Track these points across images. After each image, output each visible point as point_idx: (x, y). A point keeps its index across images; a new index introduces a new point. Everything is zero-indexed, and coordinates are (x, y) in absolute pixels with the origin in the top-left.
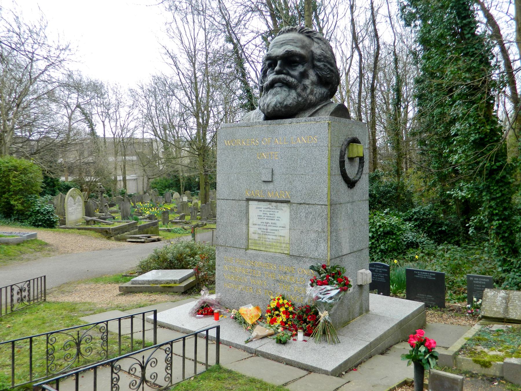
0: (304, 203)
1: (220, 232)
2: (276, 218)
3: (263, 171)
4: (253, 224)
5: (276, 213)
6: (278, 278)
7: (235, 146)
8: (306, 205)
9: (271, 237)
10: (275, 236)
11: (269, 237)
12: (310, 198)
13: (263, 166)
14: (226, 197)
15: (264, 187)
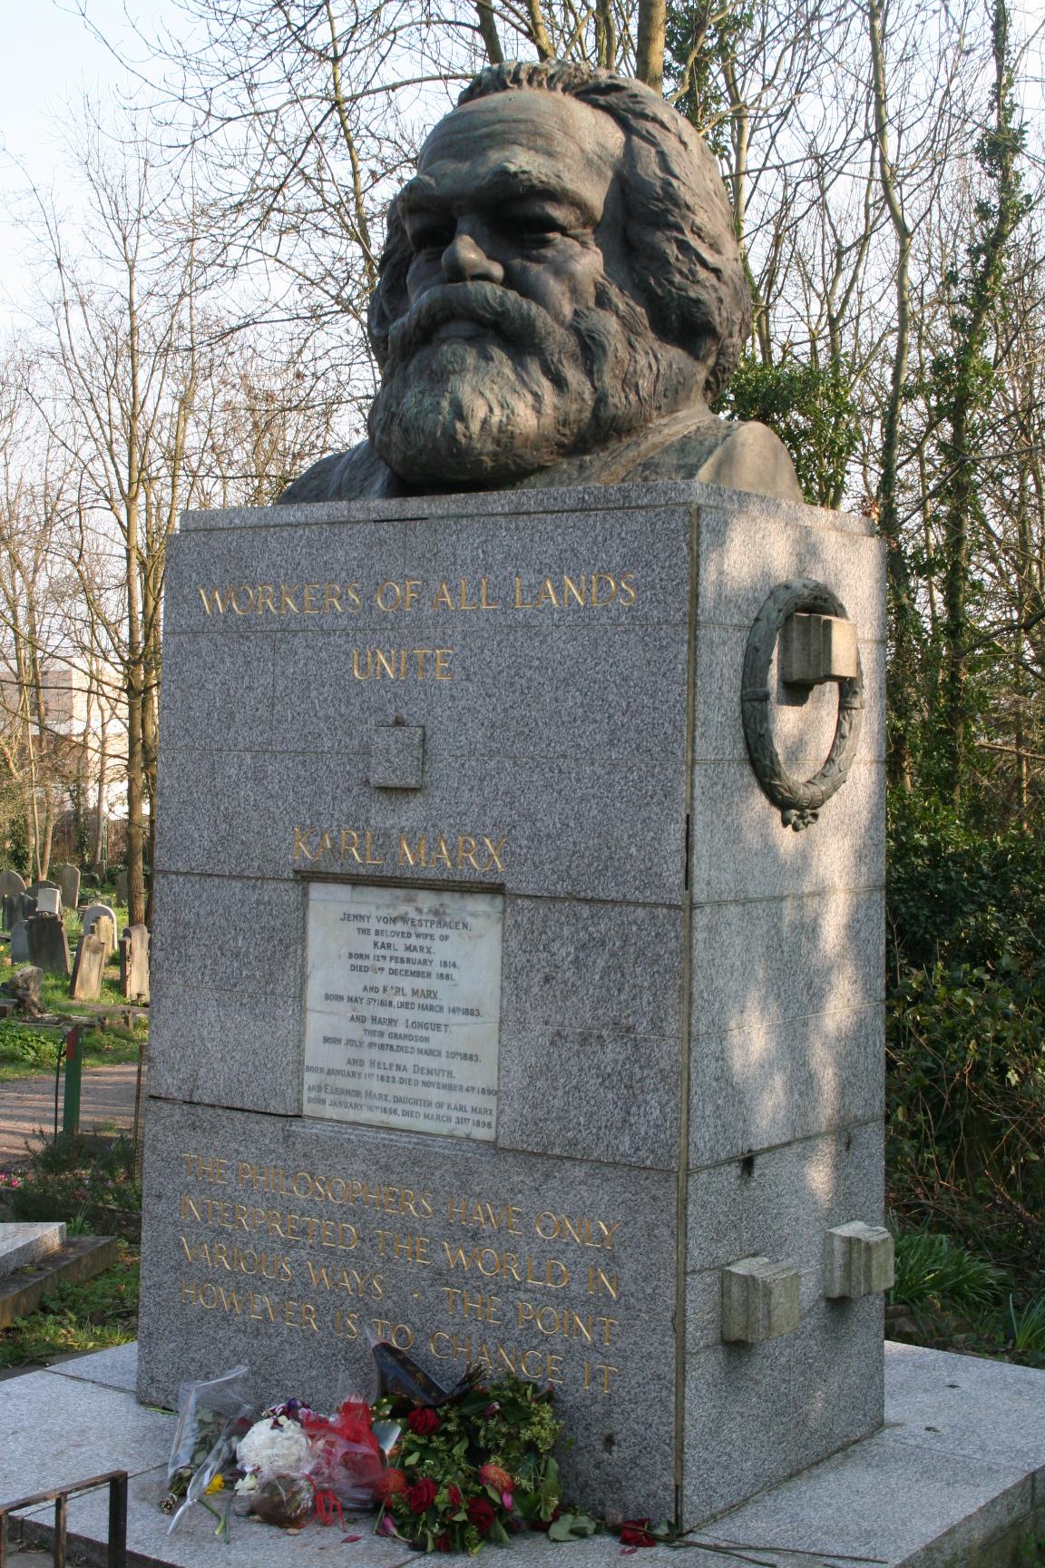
0: (573, 898)
2: (436, 969)
4: (327, 997)
5: (436, 944)
7: (246, 619)
9: (408, 1060)
10: (430, 1053)
12: (600, 873)
13: (380, 716)
15: (382, 816)
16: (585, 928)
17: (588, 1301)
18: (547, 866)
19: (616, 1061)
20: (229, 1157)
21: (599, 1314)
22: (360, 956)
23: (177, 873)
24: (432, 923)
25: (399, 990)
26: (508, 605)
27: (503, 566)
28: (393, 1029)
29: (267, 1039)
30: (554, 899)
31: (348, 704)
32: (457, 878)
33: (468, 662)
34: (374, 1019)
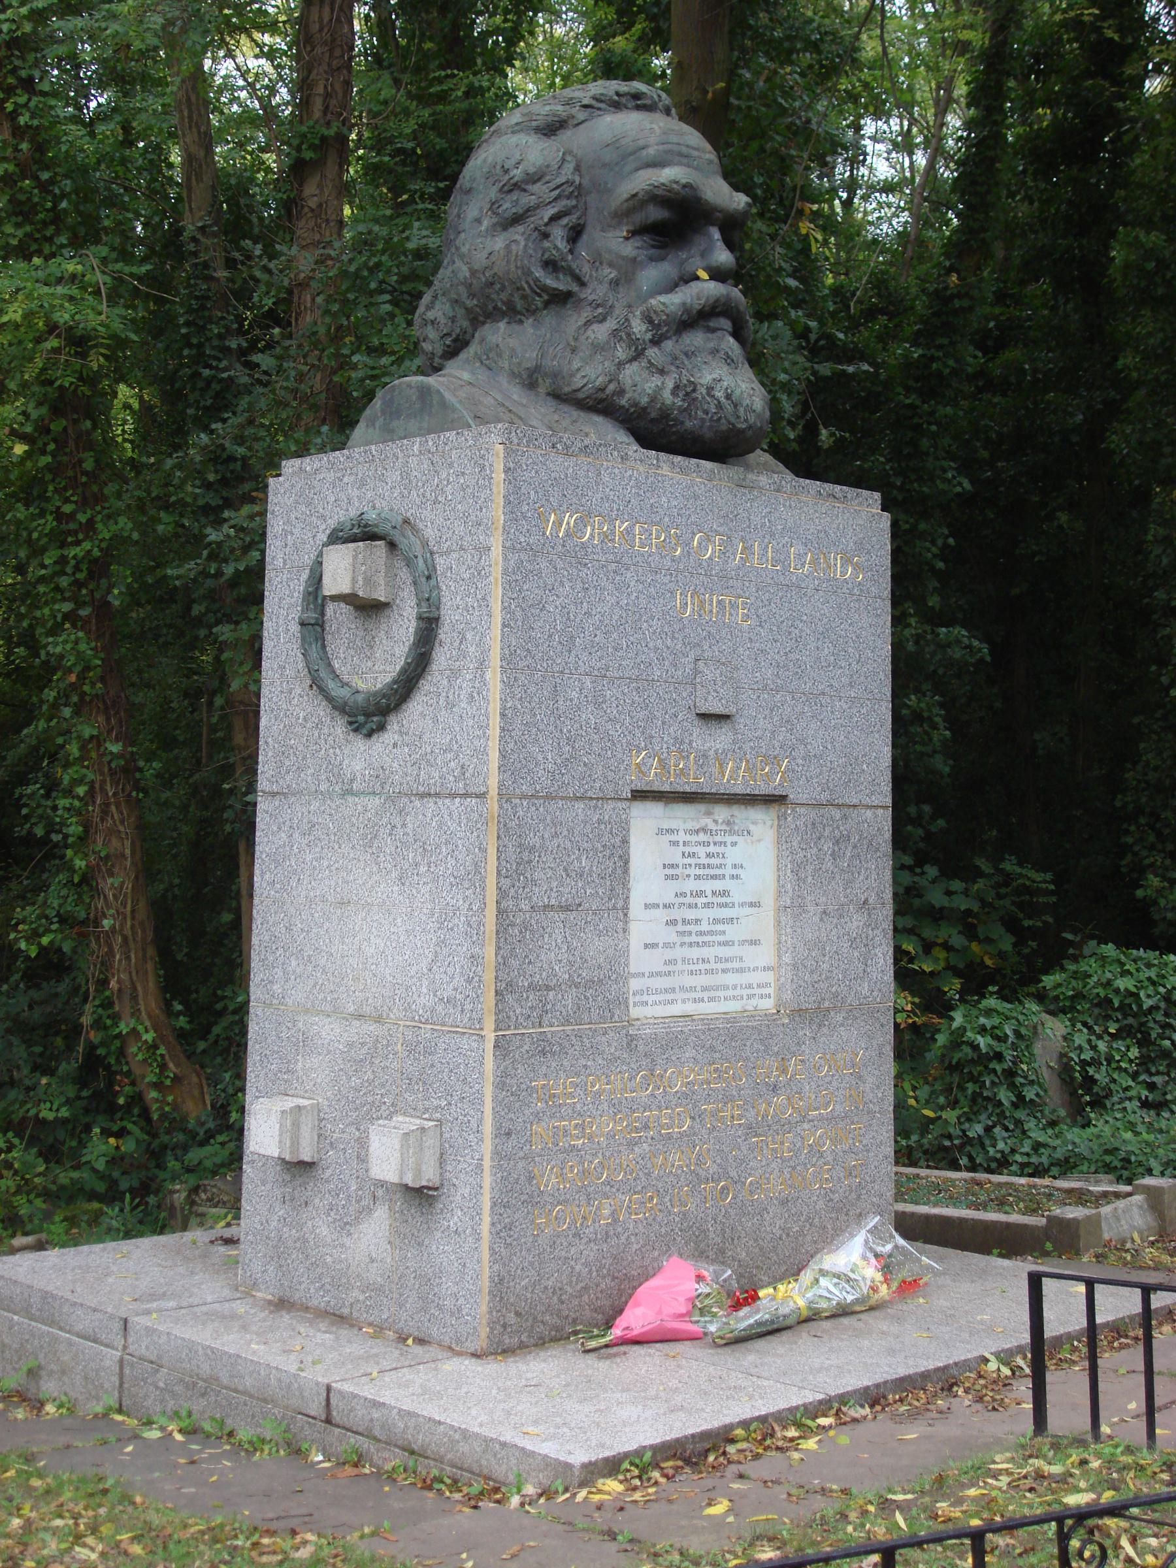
1: (514, 963)
2: (729, 871)
4: (647, 906)
5: (728, 850)
11: (706, 952)
20: (578, 1075)
22: (672, 866)
23: (523, 797)
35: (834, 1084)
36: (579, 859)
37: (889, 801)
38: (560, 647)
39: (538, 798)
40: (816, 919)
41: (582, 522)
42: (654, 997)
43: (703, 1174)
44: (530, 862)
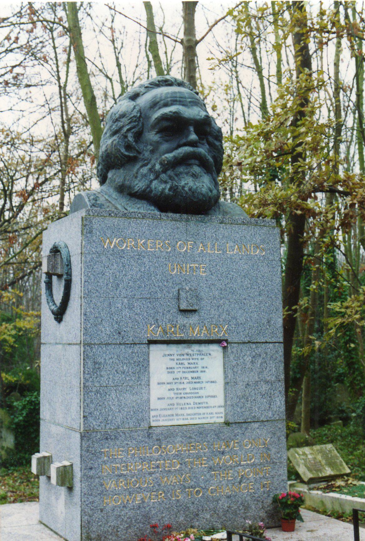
0: (249, 342)
2: (200, 369)
3: (182, 294)
5: (200, 362)
6: (211, 463)
8: (251, 345)
10: (200, 397)
13: (180, 286)
14: (105, 339)
15: (182, 320)
16: (254, 351)
17: (261, 464)
18: (241, 333)
19: (266, 390)
20: (123, 447)
21: (265, 467)
24: (198, 354)
25: (186, 378)
26: (224, 252)
27: (222, 239)
28: (185, 391)
29: (139, 401)
30: (244, 343)
31: (167, 282)
32: (211, 339)
33: (212, 269)
34: (177, 389)
35: (255, 451)
36: (123, 367)
37: (281, 340)
38: (112, 288)
39: (102, 344)
40: (243, 387)
41: (122, 242)
42: (163, 418)
43: (187, 485)
44: (99, 368)
